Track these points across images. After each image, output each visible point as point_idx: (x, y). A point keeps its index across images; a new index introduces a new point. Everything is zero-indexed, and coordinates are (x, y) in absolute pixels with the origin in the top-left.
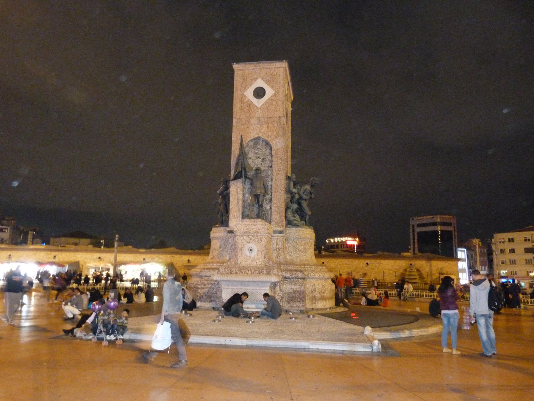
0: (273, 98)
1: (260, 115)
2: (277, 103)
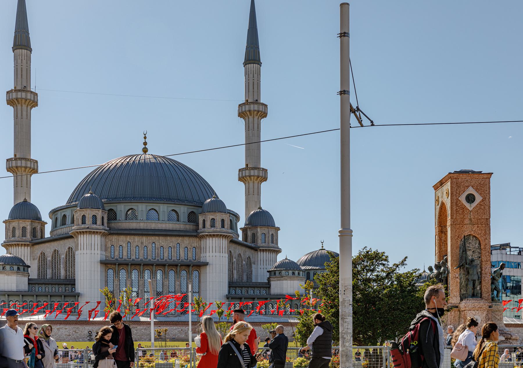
0: (481, 203)
1: (472, 216)
2: (484, 207)
